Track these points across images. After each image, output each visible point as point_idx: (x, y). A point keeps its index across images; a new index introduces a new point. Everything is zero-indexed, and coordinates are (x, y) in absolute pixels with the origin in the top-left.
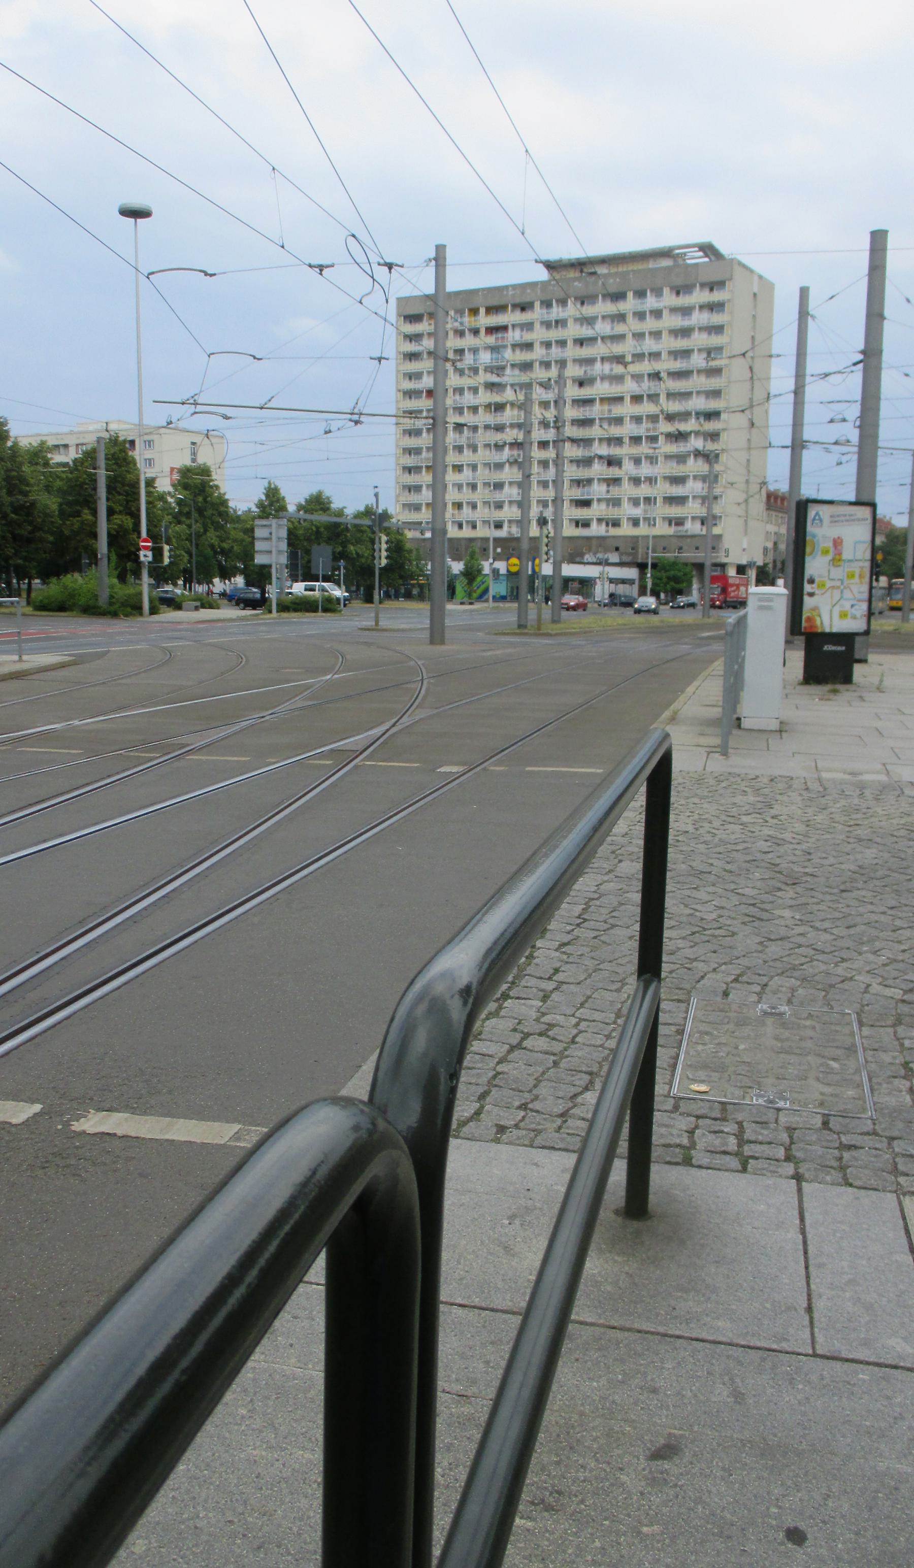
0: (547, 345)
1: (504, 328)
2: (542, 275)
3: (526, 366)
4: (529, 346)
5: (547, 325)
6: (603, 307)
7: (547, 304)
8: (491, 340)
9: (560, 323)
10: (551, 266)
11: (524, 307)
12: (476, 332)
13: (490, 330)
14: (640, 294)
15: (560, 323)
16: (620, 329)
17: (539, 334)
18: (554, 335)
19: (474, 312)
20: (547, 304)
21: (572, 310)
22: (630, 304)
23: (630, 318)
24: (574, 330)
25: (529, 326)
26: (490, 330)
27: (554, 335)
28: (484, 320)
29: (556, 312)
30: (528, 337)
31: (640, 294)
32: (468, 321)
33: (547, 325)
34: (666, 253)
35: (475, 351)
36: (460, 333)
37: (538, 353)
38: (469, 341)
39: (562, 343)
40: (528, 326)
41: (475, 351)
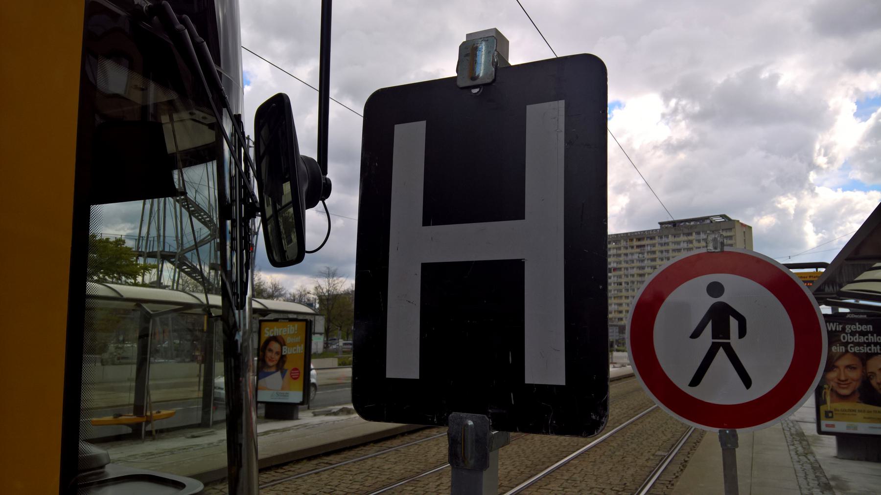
0: (662, 252)
1: (644, 246)
2: (658, 227)
3: (653, 260)
4: (654, 252)
5: (661, 245)
6: (683, 238)
7: (661, 238)
8: (638, 250)
9: (667, 244)
10: (661, 224)
11: (652, 238)
12: (632, 247)
13: (638, 247)
14: (698, 233)
15: (667, 244)
16: (690, 246)
17: (658, 248)
18: (664, 248)
19: (632, 240)
20: (661, 238)
21: (671, 239)
22: (694, 237)
23: (694, 242)
24: (672, 247)
25: (654, 245)
26: (638, 247)
27: (664, 248)
28: (635, 243)
29: (664, 240)
30: (653, 249)
31: (698, 233)
32: (629, 243)
33: (661, 245)
34: (708, 218)
35: (632, 254)
36: (626, 248)
37: (658, 255)
38: (629, 251)
39: (667, 251)
40: (654, 245)
41: (632, 254)
